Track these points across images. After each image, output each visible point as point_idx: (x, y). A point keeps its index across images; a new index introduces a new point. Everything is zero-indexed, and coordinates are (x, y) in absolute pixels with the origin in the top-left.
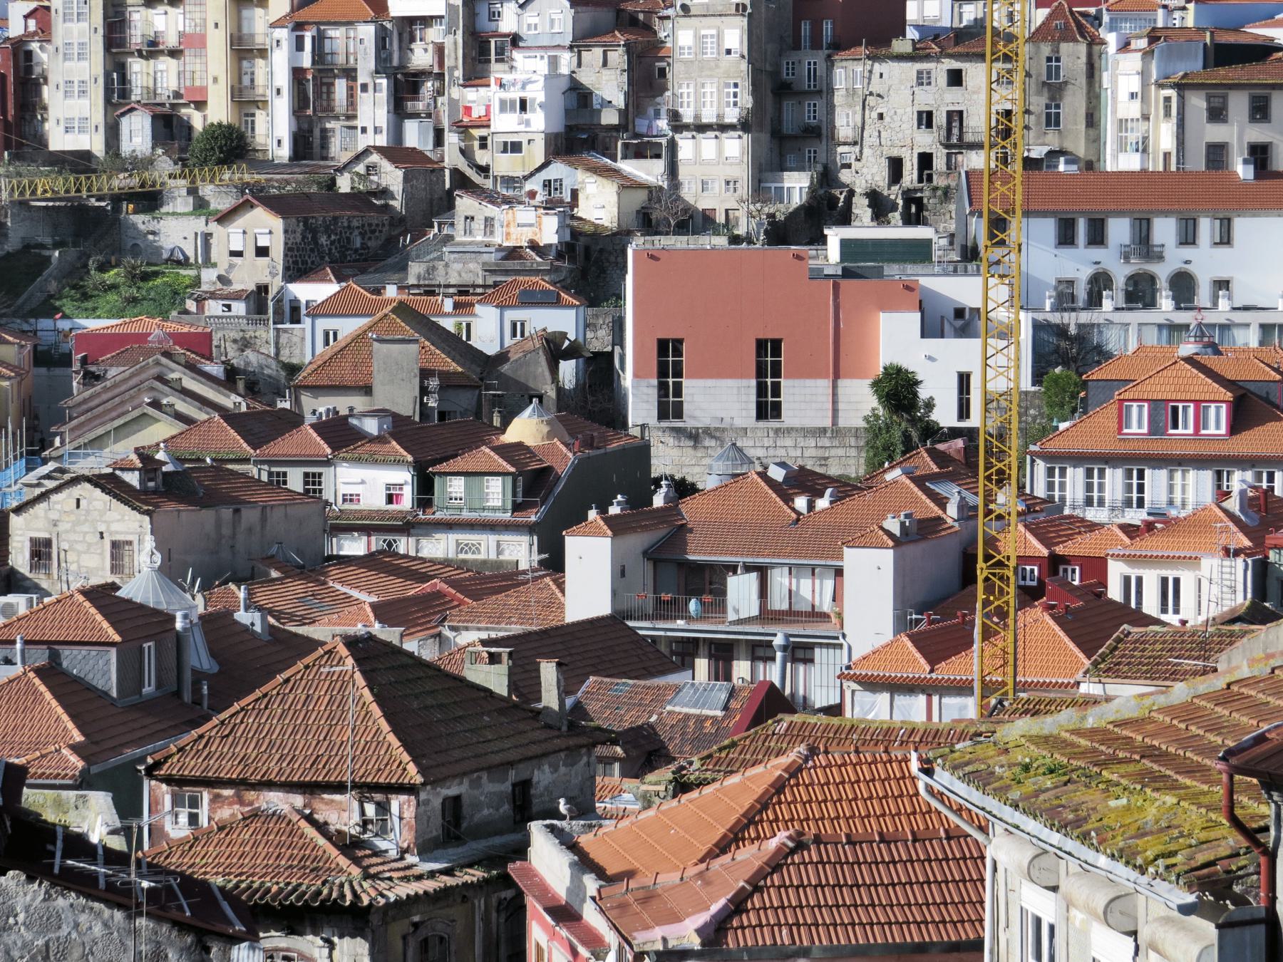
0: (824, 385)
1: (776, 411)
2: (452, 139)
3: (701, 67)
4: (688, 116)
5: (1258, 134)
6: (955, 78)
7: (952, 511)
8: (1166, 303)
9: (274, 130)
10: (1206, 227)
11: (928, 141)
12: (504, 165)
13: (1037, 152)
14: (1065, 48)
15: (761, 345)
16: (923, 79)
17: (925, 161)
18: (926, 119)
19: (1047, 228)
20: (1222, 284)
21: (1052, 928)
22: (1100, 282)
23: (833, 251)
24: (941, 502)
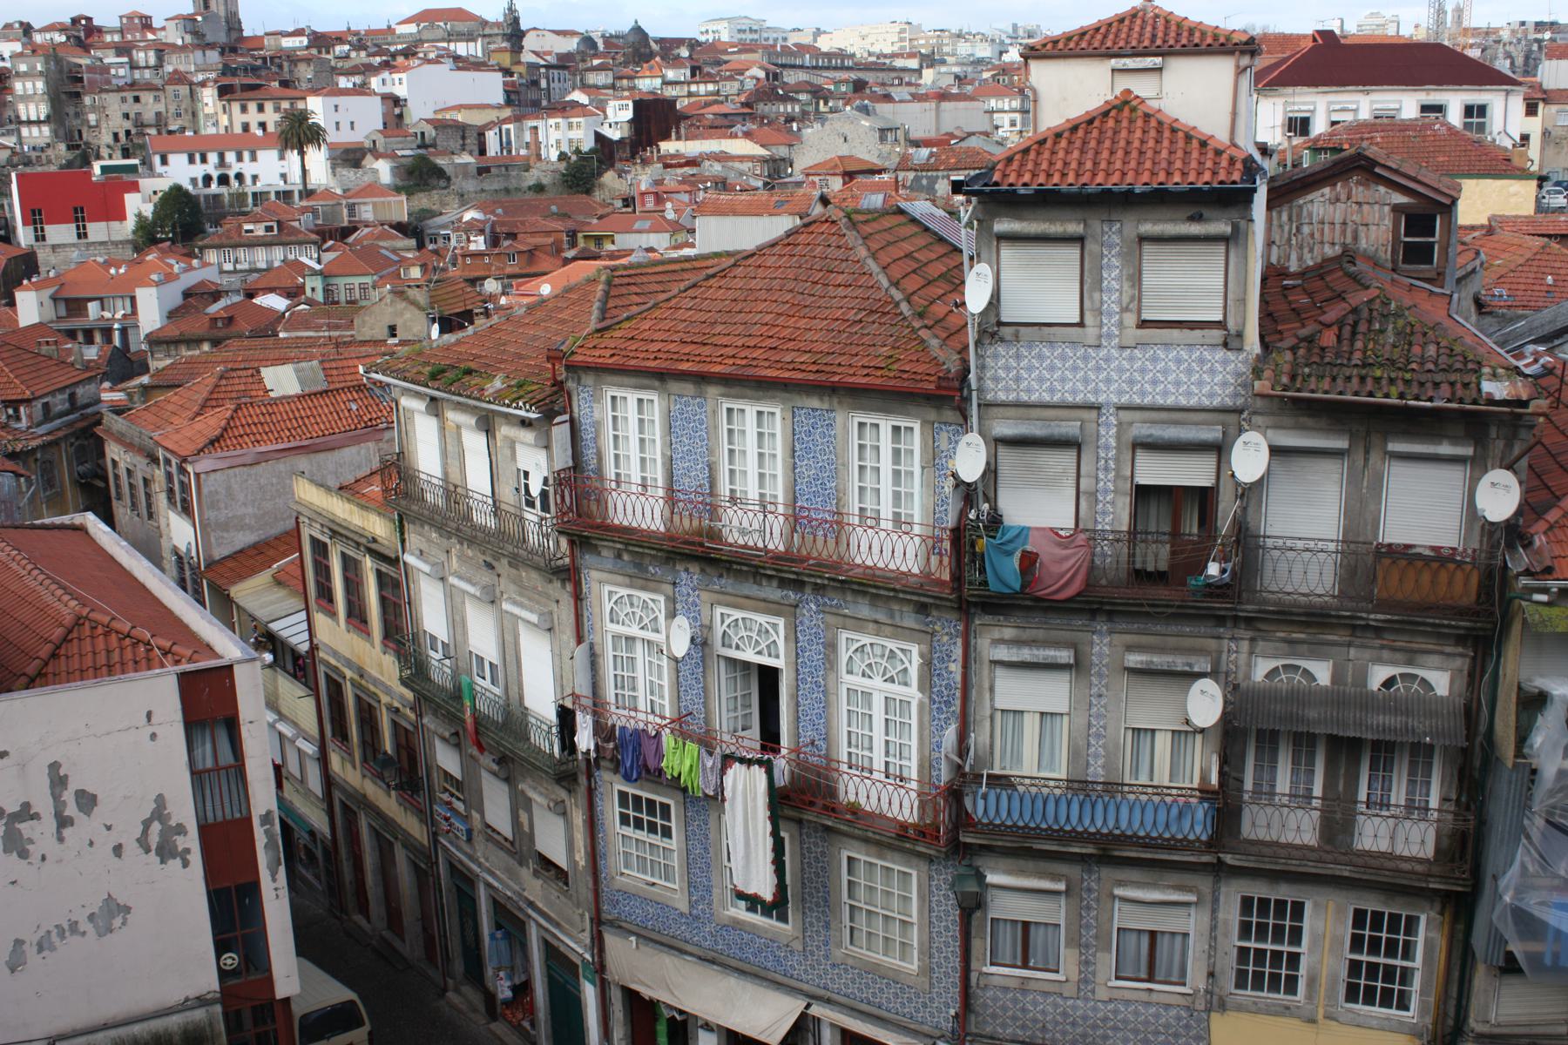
0: (103, 224)
1: (85, 235)
3: (26, 98)
4: (24, 118)
5: (261, 117)
6: (137, 99)
8: (235, 184)
10: (246, 155)
11: (128, 125)
13: (172, 128)
16: (124, 100)
17: (128, 133)
18: (126, 116)
19: (185, 157)
20: (255, 178)
22: (207, 179)
23: (97, 169)
24: (171, 266)
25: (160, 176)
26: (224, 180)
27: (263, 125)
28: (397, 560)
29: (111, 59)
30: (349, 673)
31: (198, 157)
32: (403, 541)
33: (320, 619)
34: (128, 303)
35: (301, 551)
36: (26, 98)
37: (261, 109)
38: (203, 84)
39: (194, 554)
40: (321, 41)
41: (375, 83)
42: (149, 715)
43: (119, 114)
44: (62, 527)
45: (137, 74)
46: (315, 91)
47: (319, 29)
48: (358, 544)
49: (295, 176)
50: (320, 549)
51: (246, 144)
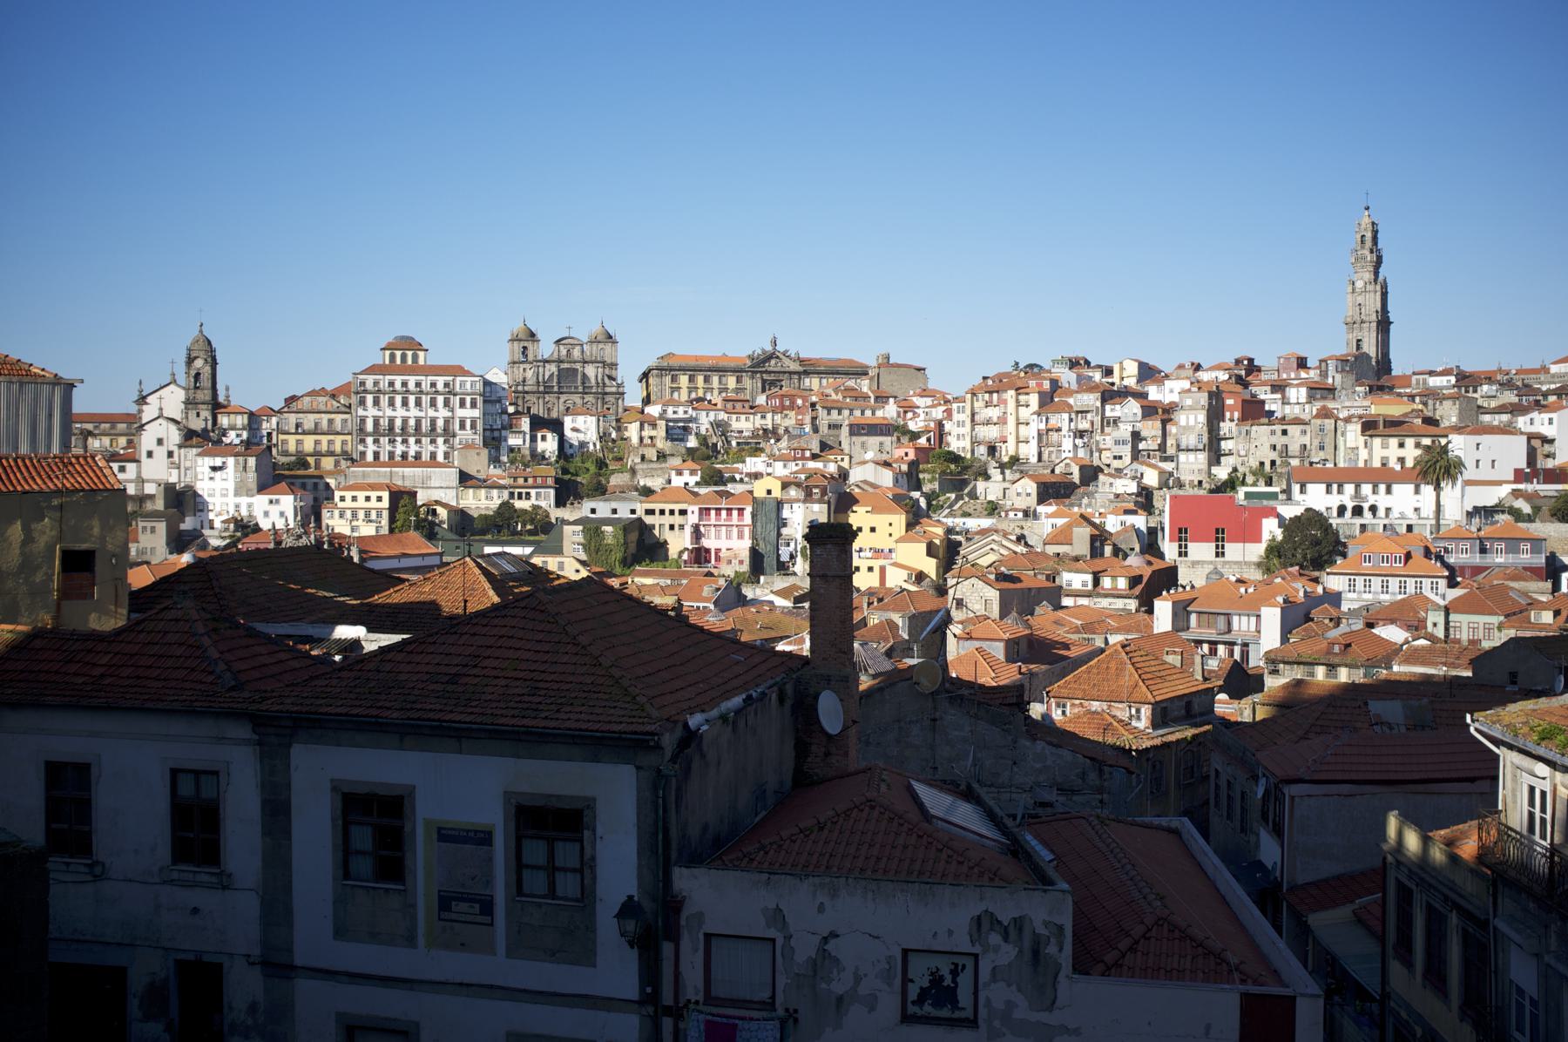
0: (1240, 545)
2: (1096, 455)
5: (1401, 453)
6: (1285, 432)
7: (1301, 594)
8: (1367, 514)
9: (1029, 451)
10: (1382, 487)
11: (1274, 455)
12: (1116, 464)
14: (1327, 421)
15: (1217, 531)
16: (1273, 433)
17: (1273, 463)
18: (1274, 447)
21: (1543, 794)
22: (1342, 510)
25: (1298, 504)
26: (1358, 511)
27: (1402, 460)
28: (1487, 921)
29: (1263, 393)
30: (1419, 1032)
31: (1335, 487)
32: (1495, 903)
33: (1396, 968)
34: (1253, 619)
35: (1384, 890)
36: (1187, 428)
37: (1401, 445)
38: (1347, 420)
39: (1278, 874)
40: (1466, 380)
41: (1522, 422)
42: (1208, 1028)
43: (1267, 446)
44: (1159, 828)
45: (1287, 409)
46: (1458, 429)
47: (1468, 368)
48: (1446, 898)
49: (1428, 510)
50: (1405, 895)
51: (1384, 477)
